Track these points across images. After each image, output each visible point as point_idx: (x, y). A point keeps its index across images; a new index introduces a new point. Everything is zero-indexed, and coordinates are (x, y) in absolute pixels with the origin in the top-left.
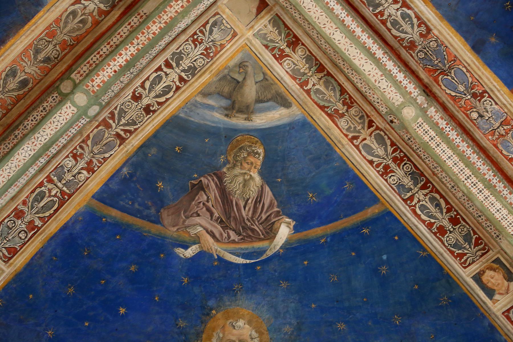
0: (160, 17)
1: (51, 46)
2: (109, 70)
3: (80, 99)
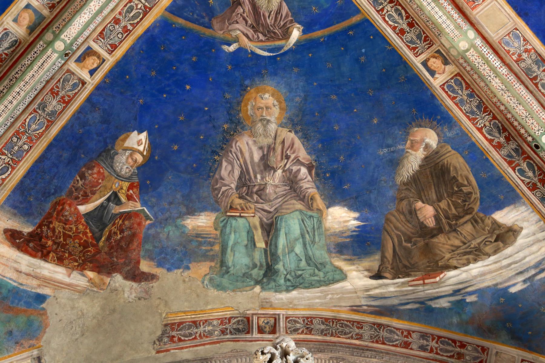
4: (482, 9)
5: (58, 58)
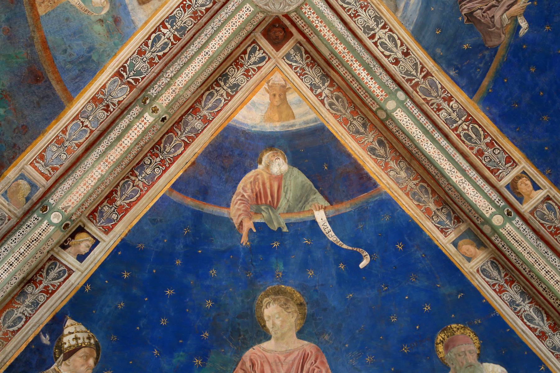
0: (332, 44)
1: (355, 122)
2: (370, 83)
3: (391, 105)
5: (512, 224)
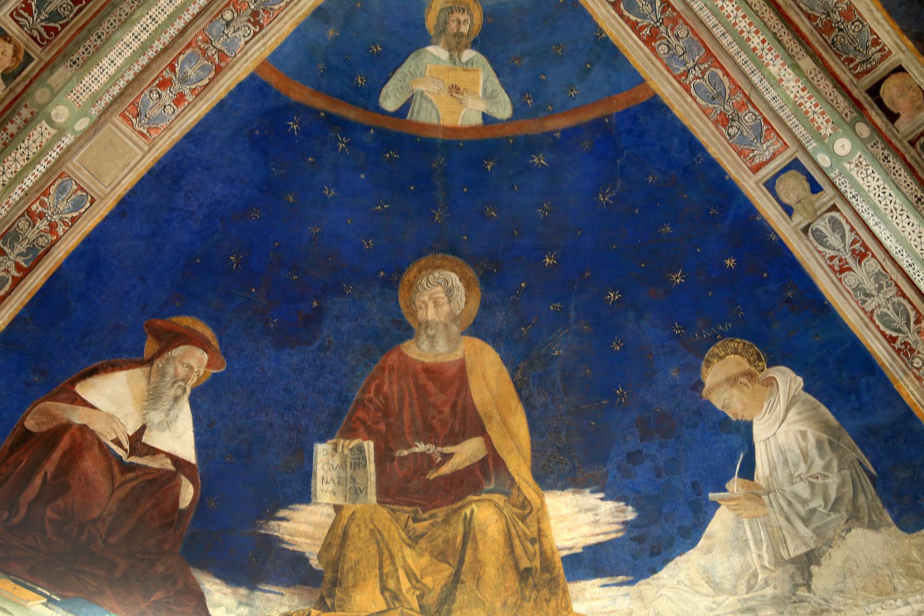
4: (124, 134)
